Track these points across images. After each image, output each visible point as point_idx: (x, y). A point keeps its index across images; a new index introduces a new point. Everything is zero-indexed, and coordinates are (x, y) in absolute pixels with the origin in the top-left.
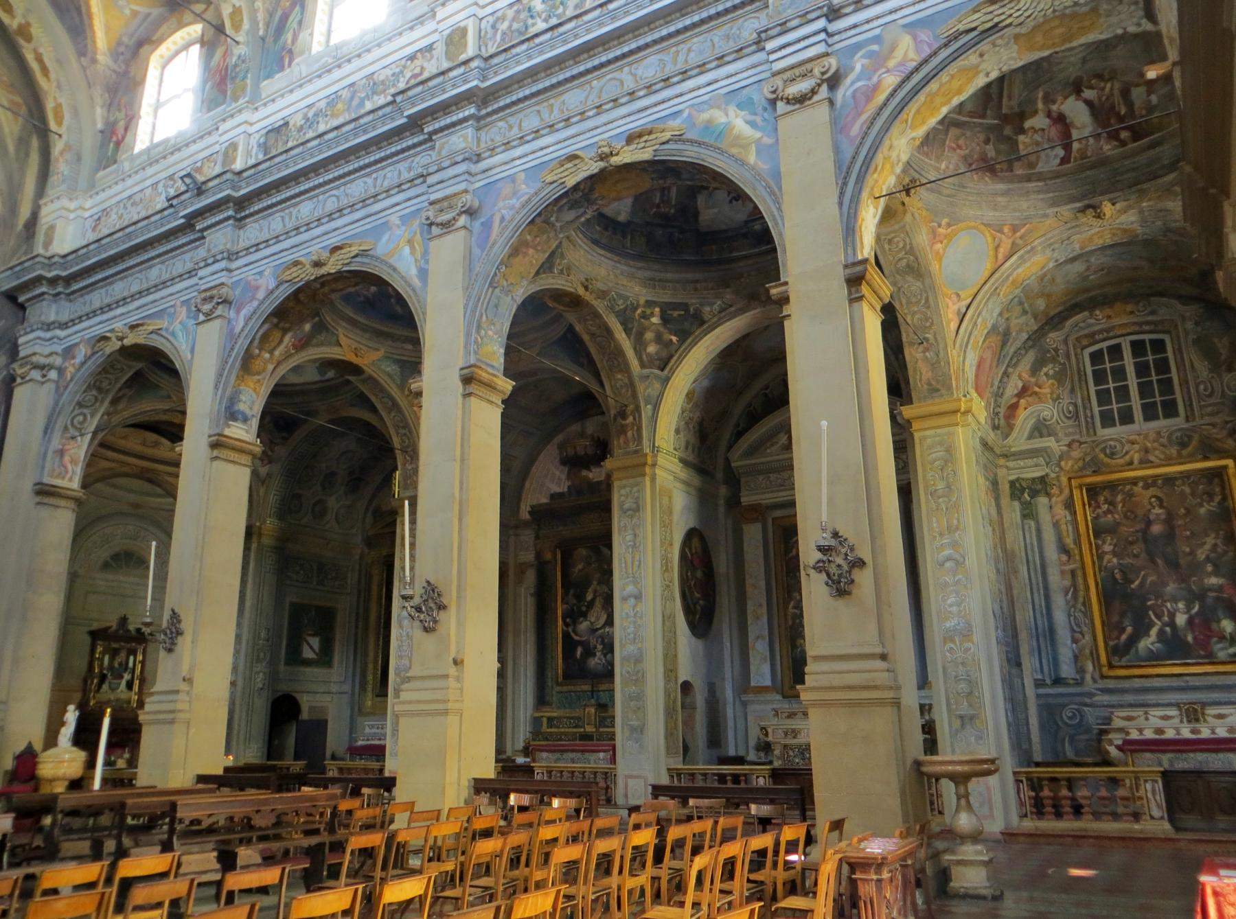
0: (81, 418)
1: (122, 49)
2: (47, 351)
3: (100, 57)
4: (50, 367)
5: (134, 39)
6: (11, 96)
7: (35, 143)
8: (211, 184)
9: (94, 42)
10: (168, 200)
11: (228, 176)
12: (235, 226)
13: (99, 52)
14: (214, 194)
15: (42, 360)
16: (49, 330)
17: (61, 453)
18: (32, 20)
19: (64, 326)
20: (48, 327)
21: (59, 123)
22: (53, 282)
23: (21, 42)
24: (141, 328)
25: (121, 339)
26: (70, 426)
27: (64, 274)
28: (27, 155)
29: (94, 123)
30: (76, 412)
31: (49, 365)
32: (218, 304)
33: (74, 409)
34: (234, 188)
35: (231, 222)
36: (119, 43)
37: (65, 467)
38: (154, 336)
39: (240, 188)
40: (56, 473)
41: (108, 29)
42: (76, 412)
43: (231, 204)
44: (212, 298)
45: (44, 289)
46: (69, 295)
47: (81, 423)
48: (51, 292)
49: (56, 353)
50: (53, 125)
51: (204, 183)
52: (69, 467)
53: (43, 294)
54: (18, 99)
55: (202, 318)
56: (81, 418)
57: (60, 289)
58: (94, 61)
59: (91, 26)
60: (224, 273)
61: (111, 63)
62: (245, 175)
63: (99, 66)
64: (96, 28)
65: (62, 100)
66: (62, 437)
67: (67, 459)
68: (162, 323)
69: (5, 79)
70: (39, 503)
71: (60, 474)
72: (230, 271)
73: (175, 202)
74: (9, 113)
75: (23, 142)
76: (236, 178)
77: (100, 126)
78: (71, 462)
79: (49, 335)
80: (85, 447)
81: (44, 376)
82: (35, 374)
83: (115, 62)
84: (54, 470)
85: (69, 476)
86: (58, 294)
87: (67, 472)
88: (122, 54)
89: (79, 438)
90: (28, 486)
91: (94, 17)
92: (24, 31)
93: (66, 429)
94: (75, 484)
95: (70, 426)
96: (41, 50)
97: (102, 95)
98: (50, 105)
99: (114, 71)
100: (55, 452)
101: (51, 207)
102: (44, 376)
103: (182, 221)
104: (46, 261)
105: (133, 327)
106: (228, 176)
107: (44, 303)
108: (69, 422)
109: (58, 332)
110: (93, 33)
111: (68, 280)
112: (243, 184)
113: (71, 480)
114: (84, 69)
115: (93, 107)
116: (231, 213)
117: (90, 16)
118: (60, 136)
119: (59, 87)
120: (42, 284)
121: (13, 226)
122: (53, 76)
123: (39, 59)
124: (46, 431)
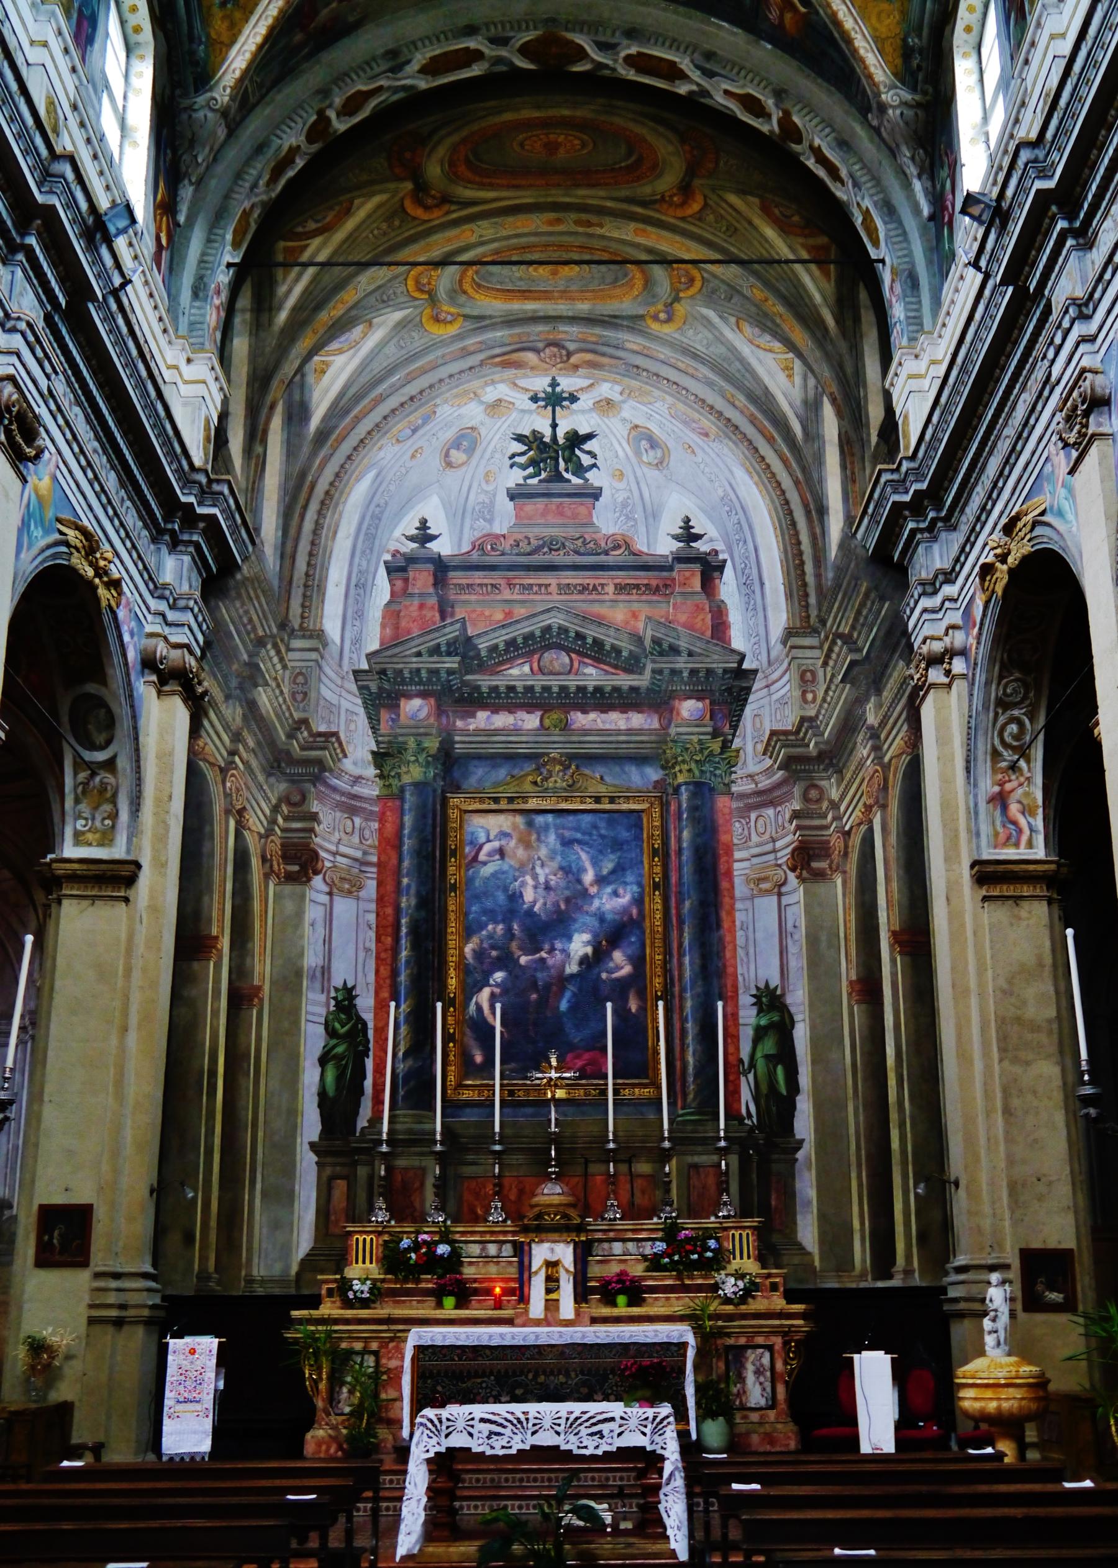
0: (1014, 728)
1: (915, 63)
2: (939, 629)
3: (886, 97)
4: (951, 653)
5: (925, 31)
6: (811, 241)
7: (863, 296)
8: (1009, 192)
9: (870, 77)
10: (975, 265)
11: (1025, 155)
12: (1079, 247)
13: (882, 88)
14: (1021, 206)
15: (937, 647)
16: (935, 592)
17: (1001, 800)
18: (787, 105)
19: (949, 576)
20: (931, 587)
21: (876, 243)
22: (917, 506)
23: (796, 148)
24: (1020, 524)
25: (1003, 558)
26: (1000, 748)
27: (924, 486)
28: (857, 320)
29: (917, 211)
30: (1002, 720)
31: (946, 651)
32: (1087, 414)
33: (996, 714)
34: (1043, 175)
35: (1070, 242)
36: (907, 53)
37: (1015, 823)
38: (1039, 531)
39: (1053, 166)
40: (1002, 837)
41: (880, 42)
42: (1002, 720)
43: (1054, 208)
44: (1075, 408)
45: (911, 525)
46: (947, 519)
47: (1016, 737)
48: (923, 525)
49: (954, 627)
50: (873, 254)
51: (1001, 195)
52: (1022, 822)
53: (913, 532)
54: (823, 240)
55: (1075, 454)
56: (1014, 728)
57: (932, 515)
58: (882, 108)
59: (855, 51)
60: (1083, 348)
61: (907, 96)
62: (1049, 135)
63: (890, 112)
64: (862, 52)
65: (867, 203)
66: (995, 771)
67: (1014, 808)
68: (1043, 500)
69: (796, 218)
70: (985, 899)
71: (1009, 838)
72: (1092, 339)
73: (983, 263)
74: (813, 267)
75: (845, 307)
76: (1041, 154)
77: (926, 211)
78: (1023, 813)
79: (937, 600)
80: (1039, 780)
81: (948, 673)
82: (936, 675)
83: (914, 89)
84: (996, 834)
85: (1024, 838)
86: (934, 521)
87: (1020, 831)
88: (919, 67)
89: (1022, 763)
90: (966, 873)
91: (853, 34)
92: (790, 132)
93: (996, 755)
94: (1039, 852)
95: (1000, 748)
96: (817, 142)
97: (913, 158)
98: (858, 220)
99: (918, 105)
100: (991, 800)
101: (900, 382)
102: (948, 673)
103: (1011, 289)
104: (895, 477)
105: (1008, 529)
106: (1025, 155)
107: (921, 550)
108: (997, 742)
109: (949, 590)
110: (862, 60)
111: (934, 494)
112: (1055, 156)
113: (1030, 845)
114: (877, 131)
115: (907, 186)
116: (1061, 224)
117: (849, 41)
118: (883, 261)
119: (856, 185)
120: (905, 518)
121: (863, 442)
122: (844, 173)
123: (822, 160)
124: (968, 770)
